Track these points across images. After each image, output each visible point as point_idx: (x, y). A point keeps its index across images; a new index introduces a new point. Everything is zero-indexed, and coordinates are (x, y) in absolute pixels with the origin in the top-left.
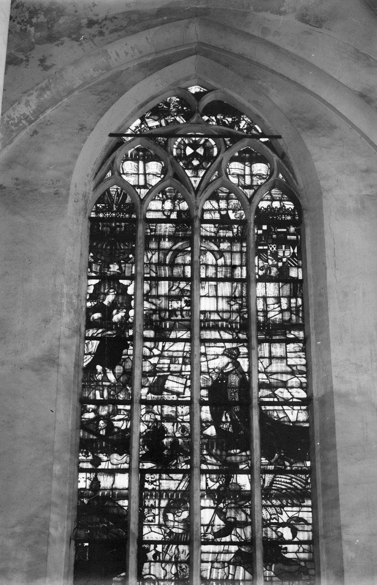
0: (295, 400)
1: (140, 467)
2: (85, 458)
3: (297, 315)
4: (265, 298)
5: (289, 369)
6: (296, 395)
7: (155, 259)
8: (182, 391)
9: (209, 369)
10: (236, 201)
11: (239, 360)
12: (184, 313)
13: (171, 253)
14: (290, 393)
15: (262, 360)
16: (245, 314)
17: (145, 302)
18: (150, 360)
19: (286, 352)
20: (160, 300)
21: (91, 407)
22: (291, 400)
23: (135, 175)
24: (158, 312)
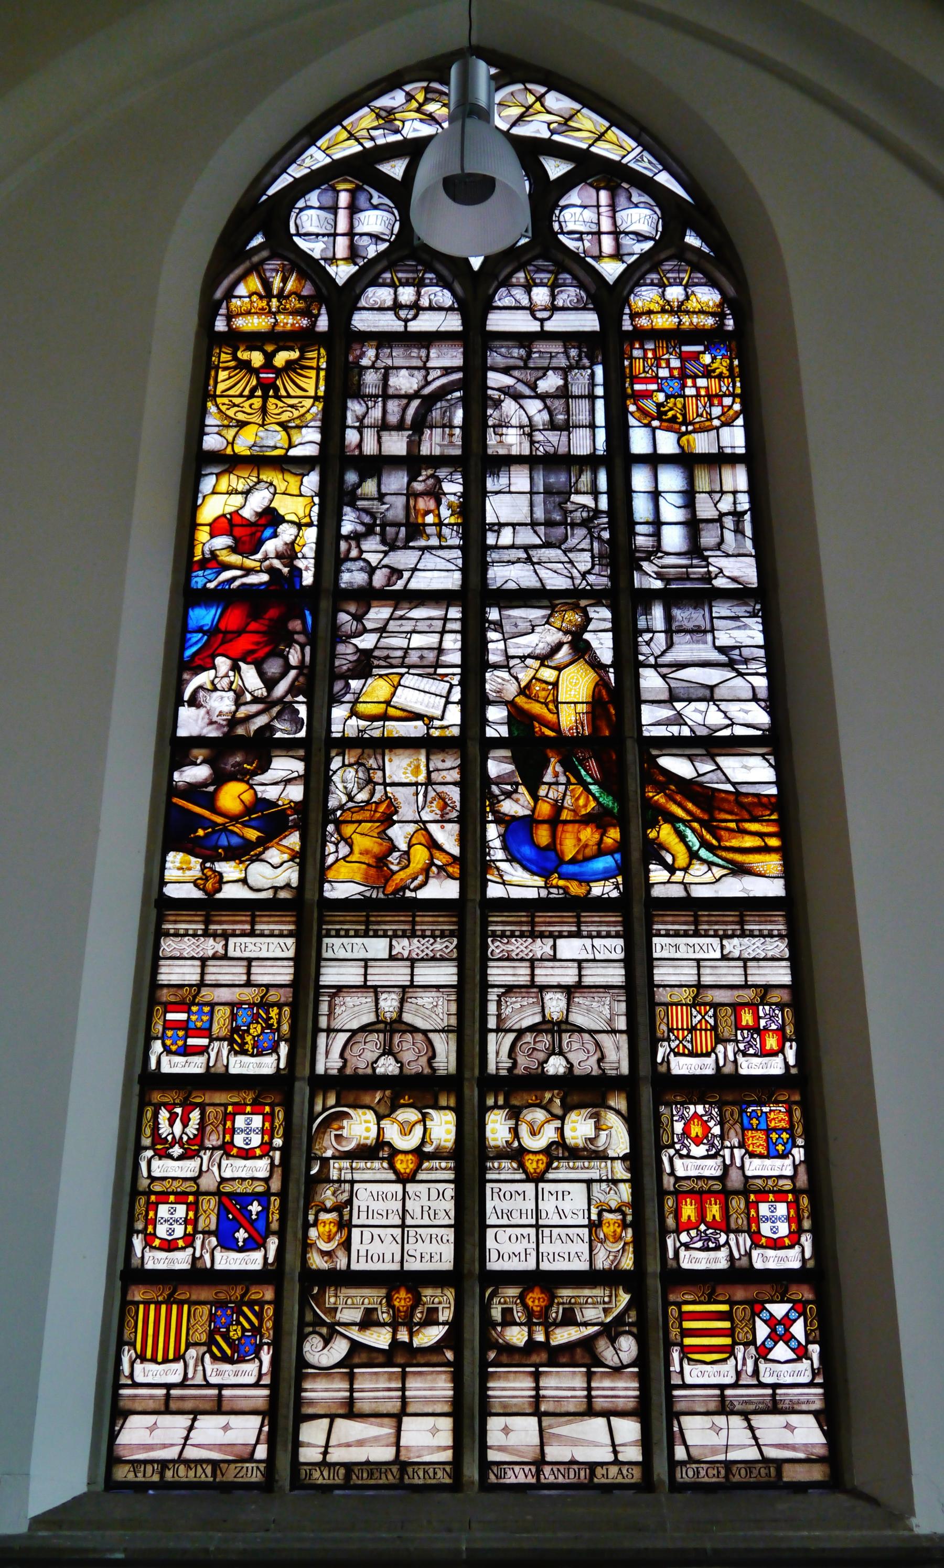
0: (740, 731)
1: (326, 894)
2: (180, 873)
3: (738, 531)
4: (655, 495)
5: (723, 658)
6: (739, 717)
7: (376, 414)
8: (438, 713)
9: (508, 658)
10: (572, 291)
11: (587, 636)
12: (446, 531)
13: (415, 403)
14: (725, 713)
15: (647, 637)
16: (604, 529)
17: (347, 509)
18: (354, 641)
19: (712, 618)
20: (384, 503)
21: (199, 754)
22: (726, 732)
23: (326, 239)
24: (378, 529)
